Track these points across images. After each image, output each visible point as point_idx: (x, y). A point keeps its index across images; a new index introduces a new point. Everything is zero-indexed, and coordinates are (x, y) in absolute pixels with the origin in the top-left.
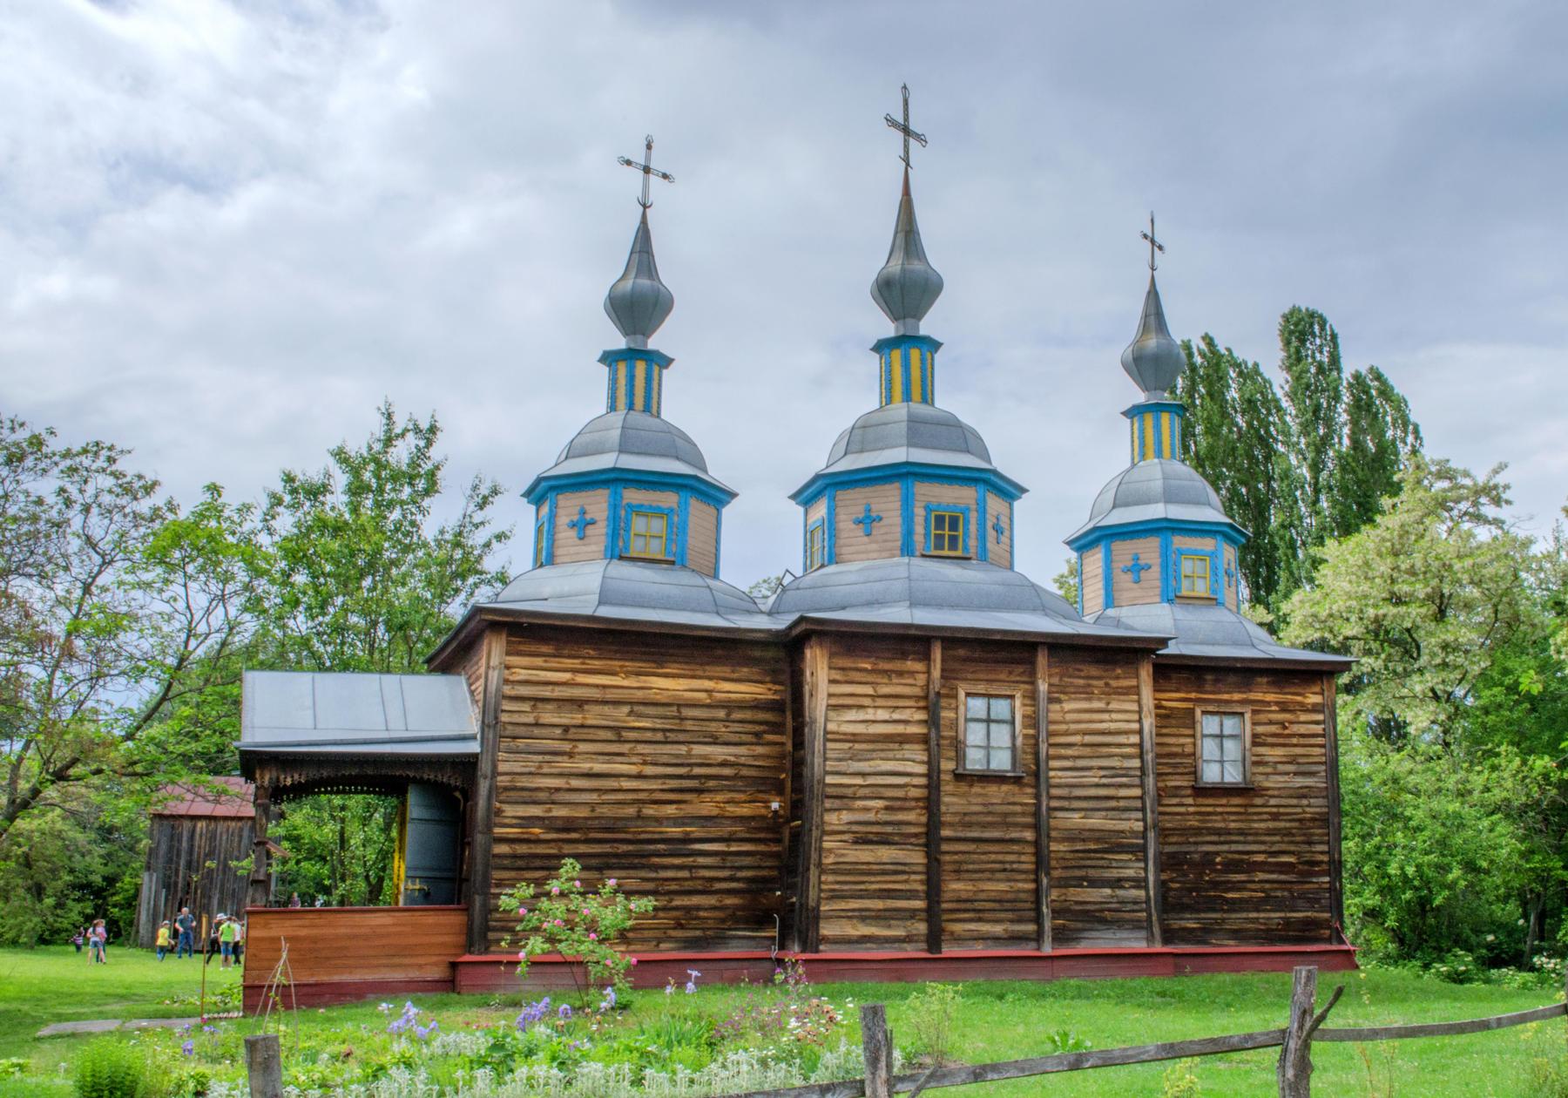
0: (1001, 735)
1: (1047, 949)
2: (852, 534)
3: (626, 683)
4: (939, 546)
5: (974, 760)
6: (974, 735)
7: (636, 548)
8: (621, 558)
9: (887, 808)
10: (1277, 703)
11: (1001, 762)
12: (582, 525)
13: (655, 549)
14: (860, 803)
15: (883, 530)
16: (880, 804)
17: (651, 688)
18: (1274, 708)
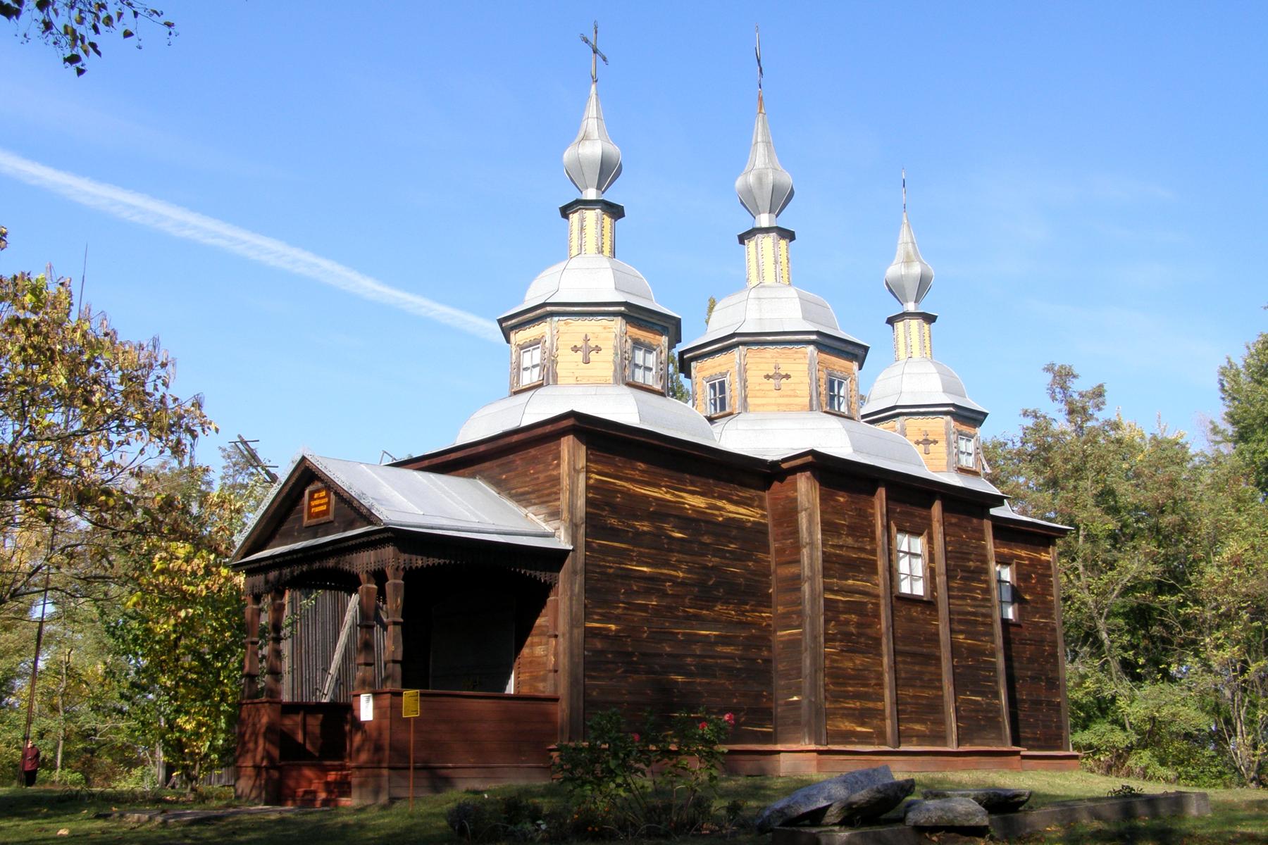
0: (919, 567)
1: (953, 748)
2: (762, 387)
3: (668, 497)
4: (831, 404)
5: (905, 588)
6: (903, 565)
7: (639, 377)
8: (630, 385)
9: (859, 625)
10: (1030, 559)
11: (919, 590)
12: (587, 350)
13: (651, 380)
14: (843, 617)
15: (793, 387)
16: (854, 617)
17: (684, 503)
18: (1027, 562)
